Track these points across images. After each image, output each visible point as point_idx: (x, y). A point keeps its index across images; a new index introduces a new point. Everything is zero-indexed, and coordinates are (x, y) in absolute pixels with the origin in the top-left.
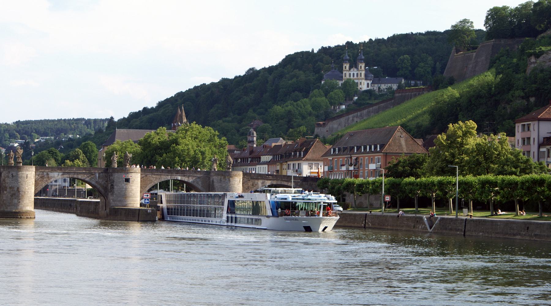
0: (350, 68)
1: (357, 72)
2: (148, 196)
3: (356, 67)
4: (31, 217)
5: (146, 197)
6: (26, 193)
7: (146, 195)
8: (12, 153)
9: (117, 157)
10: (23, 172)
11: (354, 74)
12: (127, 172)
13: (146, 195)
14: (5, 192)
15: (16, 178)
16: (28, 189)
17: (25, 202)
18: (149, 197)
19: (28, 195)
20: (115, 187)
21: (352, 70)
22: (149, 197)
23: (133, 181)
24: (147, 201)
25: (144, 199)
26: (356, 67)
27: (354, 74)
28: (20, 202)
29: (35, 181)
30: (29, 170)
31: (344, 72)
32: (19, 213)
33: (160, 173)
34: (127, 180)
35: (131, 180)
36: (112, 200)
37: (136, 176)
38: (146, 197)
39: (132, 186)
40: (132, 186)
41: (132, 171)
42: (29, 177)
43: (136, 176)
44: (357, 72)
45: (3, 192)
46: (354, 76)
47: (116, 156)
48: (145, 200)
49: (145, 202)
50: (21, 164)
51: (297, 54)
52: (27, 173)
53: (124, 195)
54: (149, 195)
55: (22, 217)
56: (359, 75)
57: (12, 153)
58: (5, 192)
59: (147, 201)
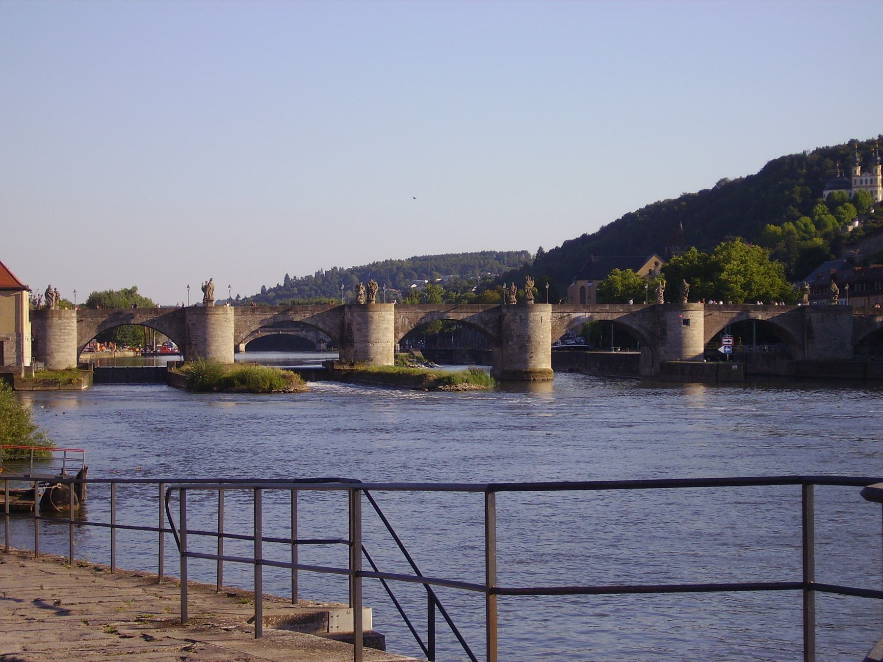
0: (862, 171)
1: (871, 178)
2: (729, 341)
3: (870, 171)
4: (549, 378)
5: (727, 343)
6: (541, 343)
7: (727, 340)
8: (514, 287)
9: (663, 289)
10: (535, 313)
11: (866, 180)
12: (684, 309)
13: (727, 340)
14: (510, 343)
15: (525, 322)
16: (543, 337)
17: (539, 357)
18: (731, 343)
19: (544, 347)
20: (668, 332)
21: (864, 175)
22: (731, 343)
23: (694, 323)
24: (727, 349)
25: (723, 347)
26: (870, 171)
27: (866, 180)
28: (532, 357)
29: (553, 327)
30: (544, 309)
31: (854, 178)
32: (531, 372)
33: (732, 310)
34: (687, 322)
35: (691, 321)
36: (663, 352)
37: (699, 315)
38: (727, 343)
39: (693, 330)
40: (693, 330)
41: (693, 309)
42: (545, 320)
43: (699, 315)
44: (871, 178)
45: (508, 343)
46: (866, 183)
47: (662, 287)
48: (725, 348)
49: (725, 351)
50: (533, 301)
51: (783, 158)
52: (542, 314)
53: (679, 343)
54: (731, 340)
55: (536, 379)
56: (874, 181)
57: (514, 287)
58: (510, 343)
59: (727, 349)
